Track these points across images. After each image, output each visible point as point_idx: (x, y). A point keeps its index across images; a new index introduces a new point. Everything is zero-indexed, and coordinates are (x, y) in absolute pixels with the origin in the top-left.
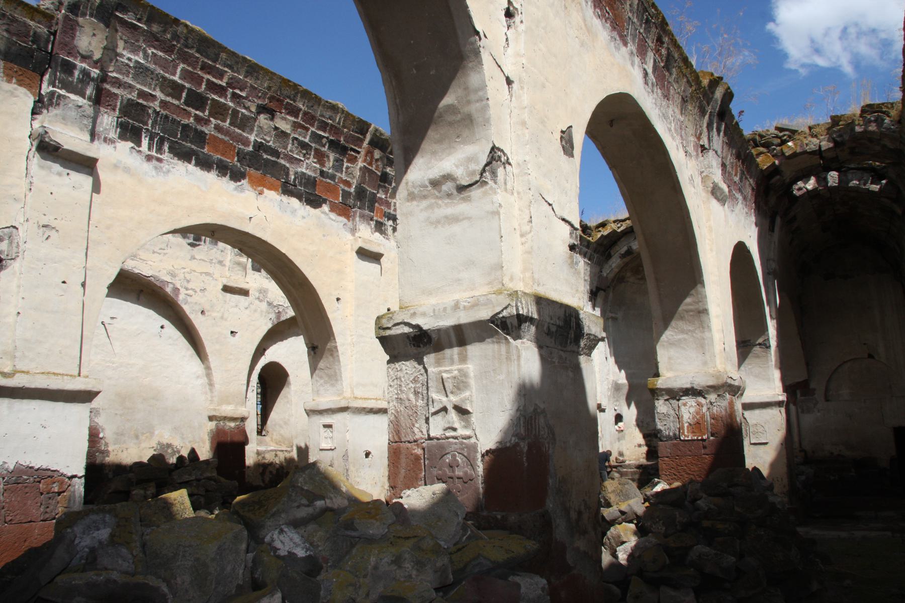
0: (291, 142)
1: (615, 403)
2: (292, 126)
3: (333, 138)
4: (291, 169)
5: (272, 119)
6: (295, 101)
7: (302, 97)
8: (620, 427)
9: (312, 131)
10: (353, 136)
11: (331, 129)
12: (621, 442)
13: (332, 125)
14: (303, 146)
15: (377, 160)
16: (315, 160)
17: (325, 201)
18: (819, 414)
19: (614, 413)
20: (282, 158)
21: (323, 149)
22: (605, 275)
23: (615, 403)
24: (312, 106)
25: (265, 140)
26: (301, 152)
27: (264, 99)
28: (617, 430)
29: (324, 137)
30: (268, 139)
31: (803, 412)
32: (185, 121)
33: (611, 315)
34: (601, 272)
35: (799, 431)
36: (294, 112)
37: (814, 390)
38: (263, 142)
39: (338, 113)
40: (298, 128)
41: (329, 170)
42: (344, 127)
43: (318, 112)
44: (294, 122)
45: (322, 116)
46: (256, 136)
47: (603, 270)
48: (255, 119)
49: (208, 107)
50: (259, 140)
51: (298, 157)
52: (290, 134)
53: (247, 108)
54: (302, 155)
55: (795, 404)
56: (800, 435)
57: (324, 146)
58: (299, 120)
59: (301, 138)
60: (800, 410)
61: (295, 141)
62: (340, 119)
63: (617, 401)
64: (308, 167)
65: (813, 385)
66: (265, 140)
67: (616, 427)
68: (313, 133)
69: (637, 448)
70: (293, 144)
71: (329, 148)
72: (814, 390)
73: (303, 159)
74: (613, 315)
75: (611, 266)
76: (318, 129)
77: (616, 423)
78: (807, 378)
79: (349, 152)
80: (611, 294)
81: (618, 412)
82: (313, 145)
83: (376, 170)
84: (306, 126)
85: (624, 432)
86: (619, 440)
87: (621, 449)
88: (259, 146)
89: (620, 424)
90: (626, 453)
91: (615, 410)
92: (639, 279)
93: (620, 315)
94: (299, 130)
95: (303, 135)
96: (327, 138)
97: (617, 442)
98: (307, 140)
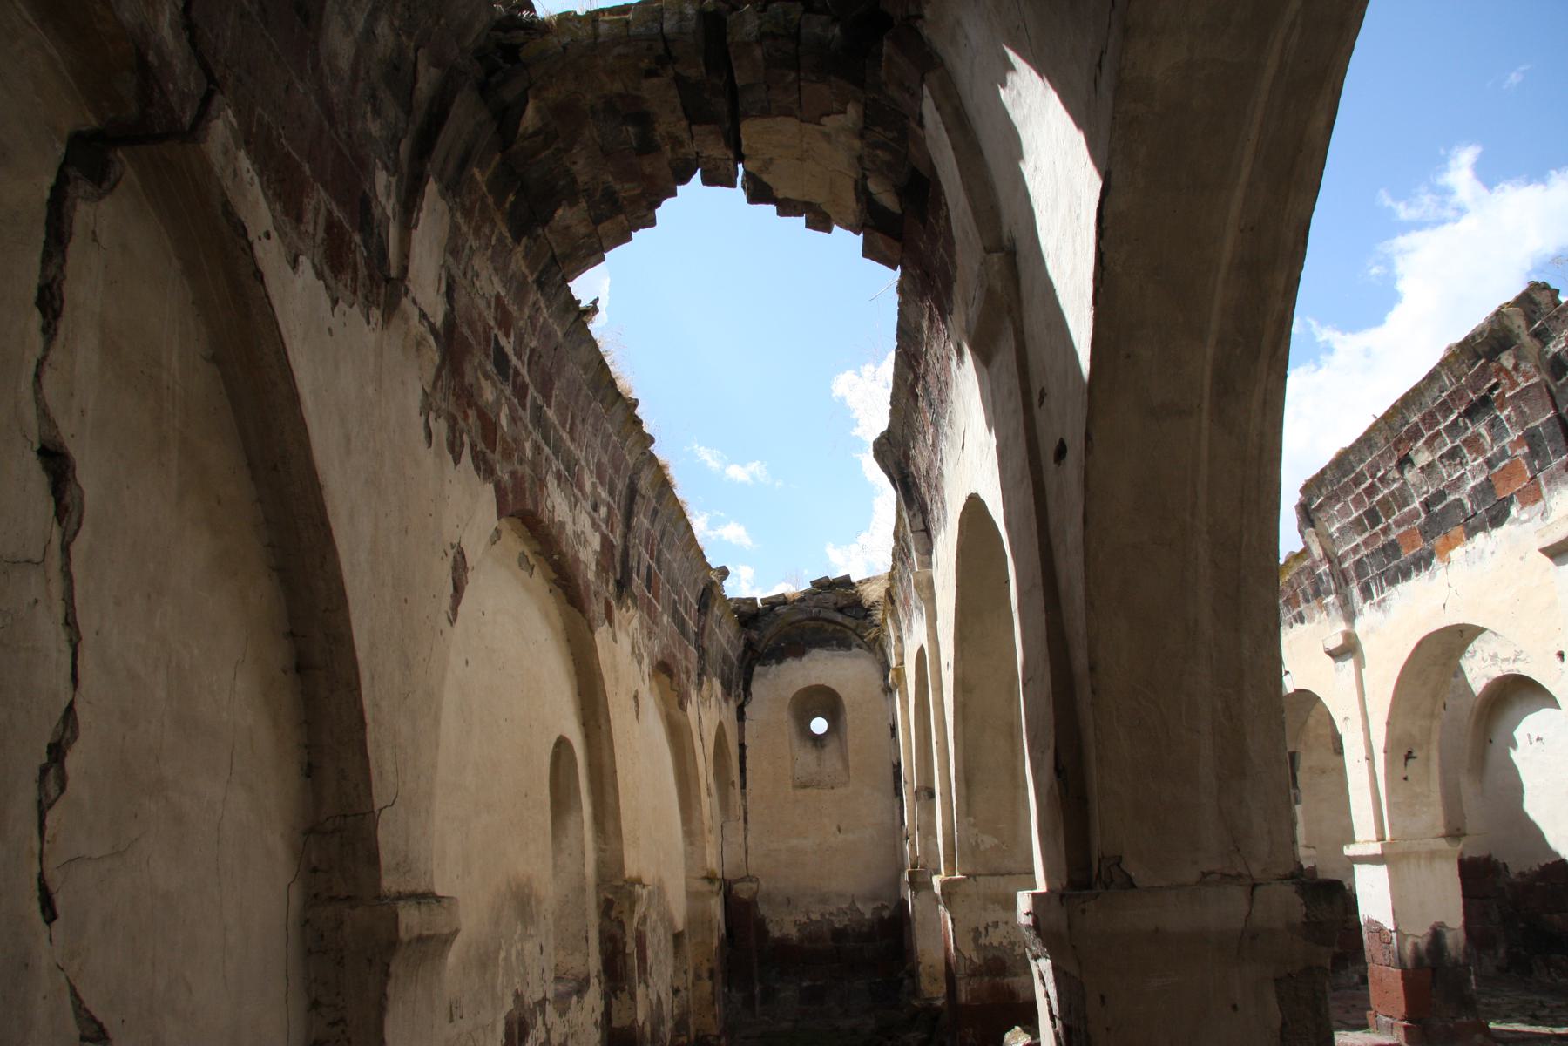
0: (1440, 466)
2: (1428, 449)
3: (1464, 408)
4: (1462, 498)
5: (1413, 465)
6: (1407, 423)
7: (1408, 410)
9: (1444, 429)
10: (1476, 374)
11: (1453, 400)
13: (1449, 396)
14: (1453, 454)
15: (1516, 367)
16: (1474, 455)
17: (1510, 500)
20: (1449, 494)
21: (1469, 433)
24: (1421, 404)
25: (1425, 493)
26: (1456, 465)
27: (1393, 454)
29: (1457, 419)
30: (1425, 489)
32: (1380, 544)
36: (1415, 434)
38: (1425, 496)
39: (1439, 373)
40: (1433, 444)
41: (1492, 449)
42: (1459, 379)
43: (1429, 403)
44: (1425, 443)
45: (1435, 400)
46: (1418, 496)
48: (1405, 483)
49: (1380, 514)
50: (1422, 499)
51: (1458, 474)
52: (1434, 460)
53: (1394, 480)
54: (1459, 467)
57: (1467, 428)
58: (1427, 434)
59: (1444, 450)
61: (1443, 460)
62: (1448, 378)
64: (1472, 473)
66: (1425, 493)
68: (1447, 429)
70: (1445, 466)
71: (1472, 421)
73: (1463, 471)
76: (1445, 418)
79: (1493, 397)
82: (1458, 442)
83: (1527, 381)
84: (1435, 431)
88: (1427, 505)
94: (1435, 444)
95: (1442, 445)
96: (1460, 415)
98: (1450, 445)
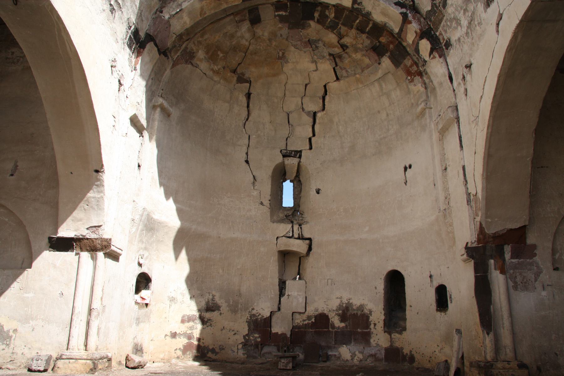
1: (141, 252)
8: (143, 299)
12: (142, 325)
18: (544, 293)
19: (139, 271)
22: (167, 17)
23: (141, 252)
28: (136, 303)
31: (515, 287)
33: (160, 101)
34: (162, 12)
35: (512, 324)
37: (534, 247)
47: (165, 10)
55: (503, 272)
56: (513, 334)
60: (511, 284)
63: (146, 249)
65: (531, 239)
67: (137, 297)
69: (168, 338)
72: (534, 247)
74: (166, 104)
75: (180, 5)
77: (137, 291)
78: (527, 223)
80: (168, 72)
81: (144, 269)
85: (149, 307)
86: (138, 321)
87: (139, 340)
89: (144, 293)
90: (147, 346)
91: (140, 265)
92: (214, 71)
93: (175, 112)
97: (134, 325)
